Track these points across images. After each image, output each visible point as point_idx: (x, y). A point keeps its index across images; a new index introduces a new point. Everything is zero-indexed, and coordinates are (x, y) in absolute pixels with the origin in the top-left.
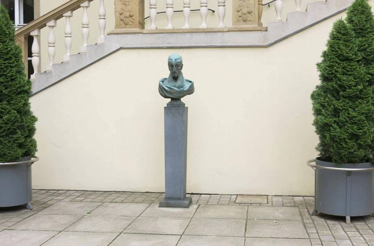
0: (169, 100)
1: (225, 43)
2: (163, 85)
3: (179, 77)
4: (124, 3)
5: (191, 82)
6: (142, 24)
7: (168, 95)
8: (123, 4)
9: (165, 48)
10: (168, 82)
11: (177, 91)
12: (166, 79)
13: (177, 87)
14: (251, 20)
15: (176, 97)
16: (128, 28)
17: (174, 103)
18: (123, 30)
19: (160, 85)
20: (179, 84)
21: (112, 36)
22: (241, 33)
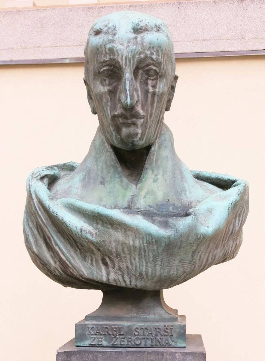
0: (97, 296)
2: (48, 203)
10: (87, 181)
12: (70, 168)
13: (148, 215)
17: (126, 324)
20: (160, 195)
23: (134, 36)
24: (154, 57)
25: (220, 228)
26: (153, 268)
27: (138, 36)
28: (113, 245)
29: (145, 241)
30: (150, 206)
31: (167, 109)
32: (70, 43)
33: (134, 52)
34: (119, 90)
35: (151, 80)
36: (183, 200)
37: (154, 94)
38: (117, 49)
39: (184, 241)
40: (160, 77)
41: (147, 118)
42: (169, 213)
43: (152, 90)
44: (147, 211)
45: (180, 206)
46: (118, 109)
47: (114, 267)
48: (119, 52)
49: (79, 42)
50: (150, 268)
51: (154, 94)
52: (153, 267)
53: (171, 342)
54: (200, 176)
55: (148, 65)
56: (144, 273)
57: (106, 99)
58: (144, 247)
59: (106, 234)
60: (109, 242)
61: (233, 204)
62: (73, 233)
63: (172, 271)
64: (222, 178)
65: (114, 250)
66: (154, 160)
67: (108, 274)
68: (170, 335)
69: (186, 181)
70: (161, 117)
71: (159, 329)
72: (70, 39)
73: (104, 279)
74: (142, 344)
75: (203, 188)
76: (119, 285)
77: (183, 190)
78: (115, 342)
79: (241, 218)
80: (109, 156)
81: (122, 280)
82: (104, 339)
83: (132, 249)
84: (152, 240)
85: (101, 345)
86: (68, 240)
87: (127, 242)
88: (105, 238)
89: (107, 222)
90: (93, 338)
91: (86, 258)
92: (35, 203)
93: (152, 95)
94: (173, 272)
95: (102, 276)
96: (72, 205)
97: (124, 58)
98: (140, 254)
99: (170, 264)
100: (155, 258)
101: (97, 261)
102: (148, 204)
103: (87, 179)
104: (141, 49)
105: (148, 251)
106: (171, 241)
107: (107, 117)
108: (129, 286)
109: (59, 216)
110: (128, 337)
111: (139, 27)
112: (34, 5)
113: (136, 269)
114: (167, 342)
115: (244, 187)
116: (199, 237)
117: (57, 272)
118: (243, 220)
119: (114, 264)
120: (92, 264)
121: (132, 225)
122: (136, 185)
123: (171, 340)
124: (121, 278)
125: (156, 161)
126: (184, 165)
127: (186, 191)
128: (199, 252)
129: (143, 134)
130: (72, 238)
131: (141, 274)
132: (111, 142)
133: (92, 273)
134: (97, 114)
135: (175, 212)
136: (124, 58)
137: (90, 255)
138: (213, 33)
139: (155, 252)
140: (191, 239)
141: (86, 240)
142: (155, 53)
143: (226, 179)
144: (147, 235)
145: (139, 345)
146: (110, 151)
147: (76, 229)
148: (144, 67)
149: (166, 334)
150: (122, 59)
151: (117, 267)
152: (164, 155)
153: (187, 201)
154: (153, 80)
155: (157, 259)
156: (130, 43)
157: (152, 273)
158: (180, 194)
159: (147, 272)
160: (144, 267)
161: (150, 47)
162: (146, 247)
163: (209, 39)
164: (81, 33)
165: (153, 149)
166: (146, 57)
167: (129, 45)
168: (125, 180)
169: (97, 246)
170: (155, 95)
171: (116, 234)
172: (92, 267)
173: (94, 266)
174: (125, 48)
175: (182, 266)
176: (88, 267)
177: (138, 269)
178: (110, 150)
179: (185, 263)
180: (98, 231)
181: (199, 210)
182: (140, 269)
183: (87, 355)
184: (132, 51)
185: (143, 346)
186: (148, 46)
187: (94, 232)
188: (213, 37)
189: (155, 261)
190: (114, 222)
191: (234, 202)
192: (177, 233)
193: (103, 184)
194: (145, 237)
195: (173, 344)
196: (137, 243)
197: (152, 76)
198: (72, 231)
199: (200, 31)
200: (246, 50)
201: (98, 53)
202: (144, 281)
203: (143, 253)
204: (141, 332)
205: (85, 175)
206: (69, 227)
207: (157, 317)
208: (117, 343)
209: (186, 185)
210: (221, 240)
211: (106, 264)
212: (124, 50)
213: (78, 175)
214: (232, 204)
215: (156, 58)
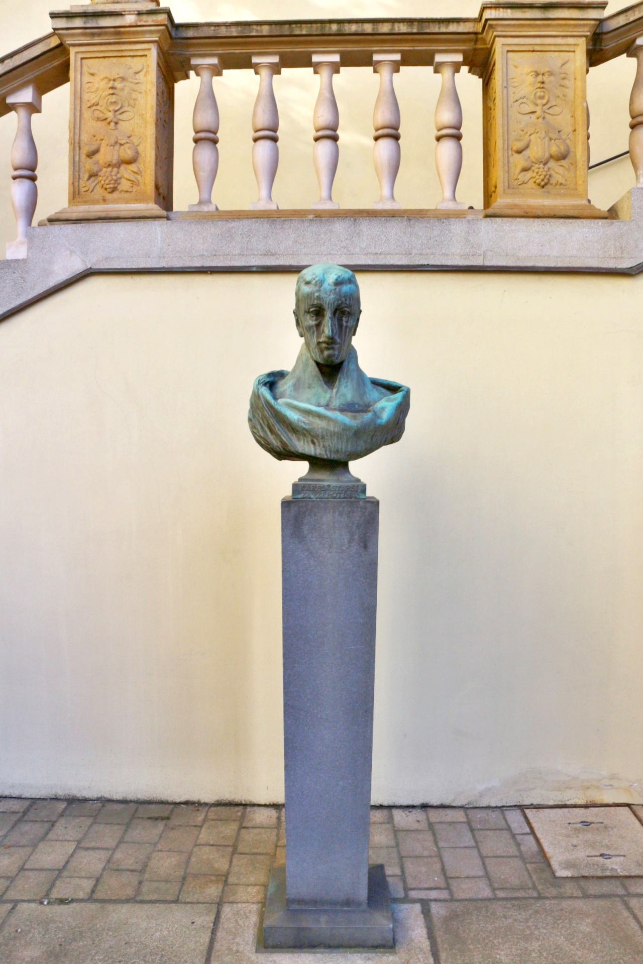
0: (303, 467)
1: (482, 257)
3: (346, 363)
4: (101, 115)
5: (393, 388)
6: (164, 198)
7: (303, 446)
8: (98, 119)
9: (254, 269)
11: (346, 428)
12: (281, 375)
13: (342, 410)
14: (561, 184)
15: (334, 456)
16: (116, 201)
17: (326, 483)
18: (98, 209)
19: (256, 397)
21: (56, 228)
22: (537, 224)
23: (334, 288)
24: (348, 302)
28: (320, 430)
29: (341, 429)
30: (342, 404)
31: (354, 334)
37: (346, 327)
40: (351, 314)
47: (319, 446)
48: (324, 299)
51: (346, 327)
53: (357, 496)
55: (343, 308)
65: (320, 434)
67: (315, 450)
73: (313, 453)
76: (323, 457)
78: (320, 495)
80: (313, 369)
87: (329, 428)
94: (359, 448)
95: (311, 451)
96: (290, 404)
97: (327, 303)
98: (338, 437)
101: (308, 442)
110: (327, 492)
111: (338, 282)
112: (217, 209)
117: (278, 448)
120: (304, 443)
122: (332, 389)
124: (324, 453)
125: (346, 373)
129: (338, 355)
132: (315, 359)
133: (304, 450)
136: (327, 303)
140: (372, 427)
142: (348, 300)
148: (341, 309)
149: (353, 490)
150: (326, 303)
151: (322, 446)
154: (346, 317)
159: (341, 449)
165: (344, 364)
166: (342, 303)
177: (336, 447)
178: (314, 364)
188: (384, 251)
189: (347, 441)
195: (358, 496)
196: (336, 430)
204: (337, 490)
205: (296, 382)
208: (322, 495)
209: (367, 390)
211: (314, 443)
212: (327, 297)
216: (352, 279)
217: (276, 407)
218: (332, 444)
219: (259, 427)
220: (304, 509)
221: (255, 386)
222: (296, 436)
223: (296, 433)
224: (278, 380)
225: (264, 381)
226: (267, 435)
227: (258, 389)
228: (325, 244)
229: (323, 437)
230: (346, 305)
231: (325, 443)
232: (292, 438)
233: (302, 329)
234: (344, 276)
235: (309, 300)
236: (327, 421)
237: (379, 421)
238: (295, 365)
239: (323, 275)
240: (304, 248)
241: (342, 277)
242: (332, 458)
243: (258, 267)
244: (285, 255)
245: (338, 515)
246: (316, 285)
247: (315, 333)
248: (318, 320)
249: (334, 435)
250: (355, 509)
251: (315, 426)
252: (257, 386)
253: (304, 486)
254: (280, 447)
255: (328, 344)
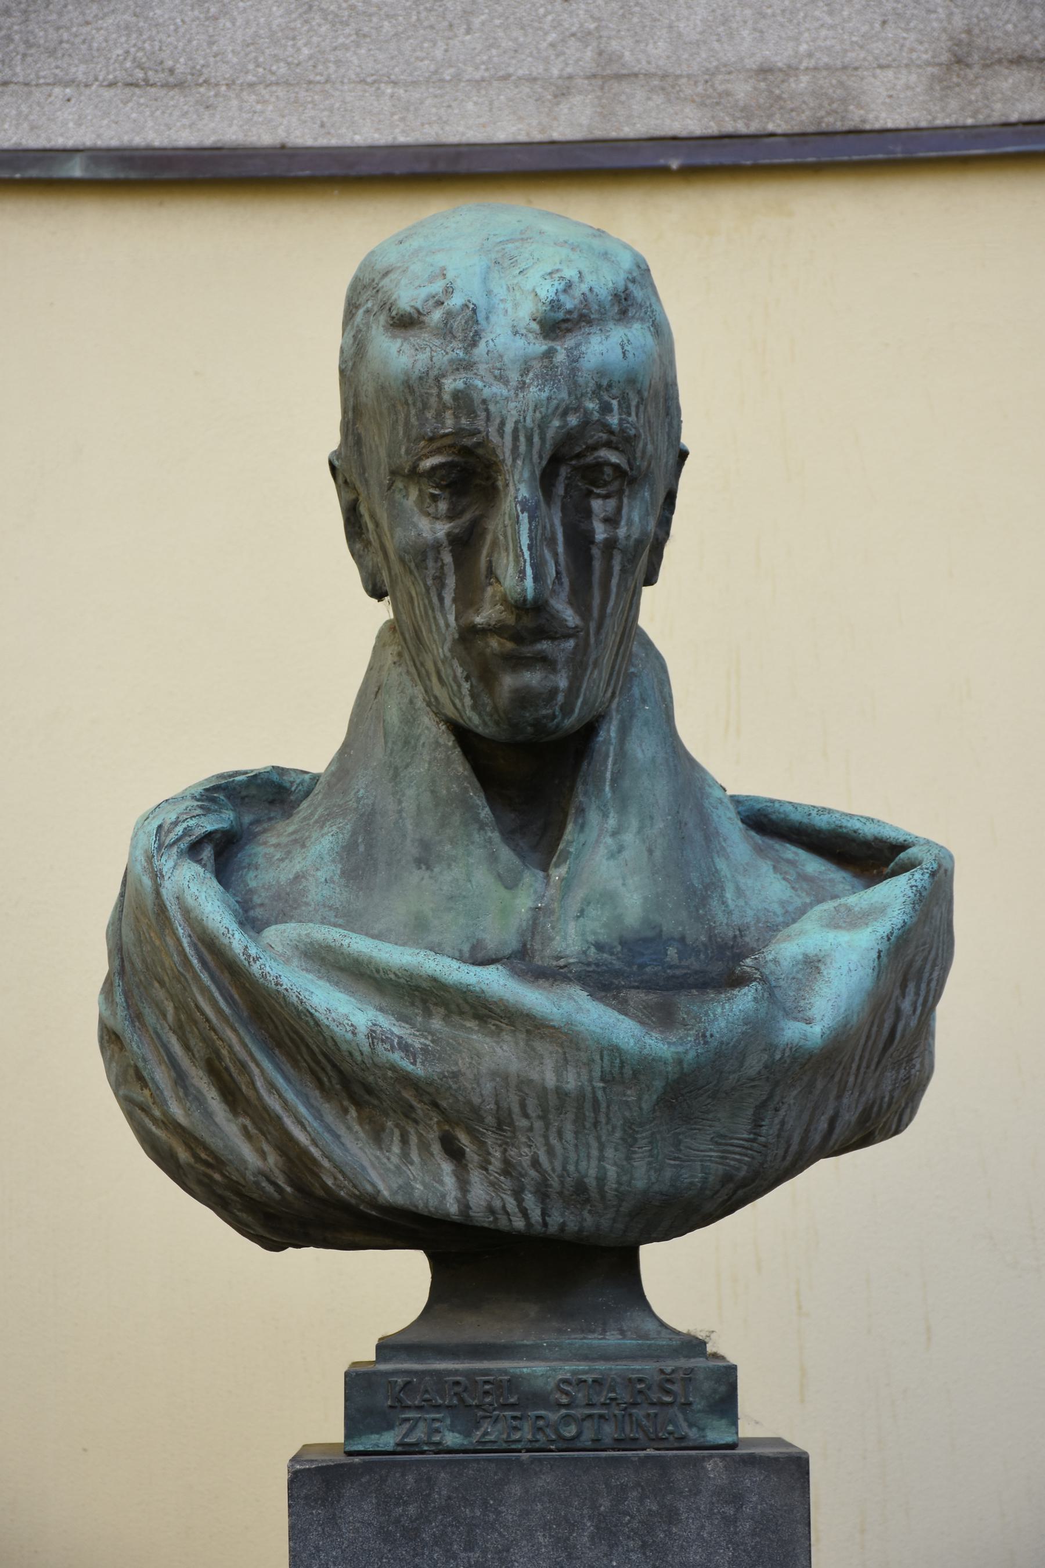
9: (76, 170)
23: (540, 347)
24: (614, 420)
25: (849, 1026)
26: (623, 1166)
27: (559, 348)
28: (488, 1087)
29: (597, 1074)
30: (600, 947)
31: (650, 579)
32: (82, 68)
33: (543, 410)
34: (489, 538)
35: (599, 496)
36: (715, 923)
38: (484, 397)
39: (729, 1073)
40: (632, 481)
41: (588, 634)
42: (668, 971)
43: (605, 536)
44: (589, 964)
45: (704, 945)
46: (487, 605)
48: (492, 408)
49: (128, 64)
50: (615, 1164)
51: (611, 544)
52: (625, 1163)
53: (685, 1429)
54: (770, 820)
56: (591, 1182)
57: (440, 564)
58: (594, 1092)
59: (460, 1052)
60: (471, 1077)
61: (893, 939)
62: (339, 1049)
63: (686, 1176)
64: (855, 832)
66: (608, 775)
68: (684, 1404)
69: (723, 848)
70: (630, 619)
71: (640, 1380)
72: (84, 47)
73: (453, 1208)
74: (583, 1438)
75: (786, 873)
76: (503, 1223)
77: (713, 884)
79: (923, 986)
81: (517, 1210)
82: (448, 1422)
83: (553, 1101)
84: (622, 1067)
85: (439, 1443)
86: (313, 1072)
87: (535, 1076)
88: (457, 1064)
89: (467, 1008)
90: (407, 1420)
91: (383, 1136)
92: (185, 942)
93: (603, 552)
94: (692, 1176)
96: (329, 948)
97: (509, 428)
98: (579, 1120)
99: (680, 1150)
100: (631, 1131)
101: (424, 1147)
102: (591, 938)
103: (362, 848)
104: (570, 394)
105: (608, 1107)
106: (685, 1070)
107: (443, 629)
108: (539, 1228)
109: (286, 990)
110: (532, 1413)
111: (561, 315)
113: (564, 1169)
114: (670, 1428)
115: (933, 874)
116: (778, 1057)
117: (270, 1189)
118: (932, 993)
119: (489, 1154)
120: (405, 1155)
121: (552, 1020)
122: (545, 868)
123: (686, 1420)
124: (511, 1204)
126: (710, 786)
127: (723, 889)
128: (777, 1110)
129: (573, 690)
130: (334, 1066)
131: (581, 1188)
132: (450, 711)
133: (407, 1188)
134: (387, 598)
135: (688, 967)
136: (509, 428)
137: (397, 1126)
138: (808, 30)
139: (631, 1109)
140: (754, 1064)
141: (390, 1073)
142: (615, 403)
143: (870, 837)
144: (605, 1052)
145: (573, 1439)
146: (446, 745)
147: (354, 1033)
148: (579, 456)
149: (668, 1399)
151: (496, 1164)
152: (640, 755)
153: (727, 924)
155: (637, 1132)
156: (531, 375)
157: (619, 1183)
158: (704, 901)
159: (601, 1180)
160: (594, 1163)
161: (599, 386)
162: (600, 1094)
163: (789, 67)
164: (135, 15)
165: (602, 736)
166: (586, 423)
167: (527, 381)
168: (506, 854)
169: (428, 1093)
170: (614, 548)
171: (498, 1050)
172: (404, 1168)
173: (412, 1163)
174: (512, 392)
175: (722, 1157)
176: (392, 1167)
177: (571, 1168)
178: (448, 740)
179: (732, 1145)
180: (433, 1041)
181: (775, 961)
182: (577, 1170)
183: (397, 1475)
184: (536, 406)
185: (589, 1444)
186: (592, 384)
187: (417, 1045)
188: (810, 55)
189: (629, 1142)
190: (491, 1010)
191: (896, 931)
192: (706, 1043)
193: (424, 867)
194: (597, 1057)
196: (571, 1082)
197: (606, 484)
198: (338, 1040)
199: (745, 22)
200: (970, 121)
201: (410, 402)
202: (590, 1212)
203: (589, 1114)
205: (354, 833)
206: (328, 1027)
207: (634, 1342)
209: (721, 864)
210: (854, 1066)
211: (454, 1152)
212: (507, 399)
213: (326, 830)
214: (889, 939)
215: (621, 420)
216: (638, 293)
217: (255, 968)
218: (551, 1152)
219: (161, 1076)
220: (412, 1510)
221: (142, 858)
222: (361, 1121)
223: (358, 1104)
224: (257, 822)
225: (187, 832)
226: (208, 1115)
227: (157, 876)
228: (477, 22)
229: (503, 1123)
230: (605, 436)
231: (512, 1152)
232: (342, 1131)
233: (380, 559)
234: (590, 280)
235: (413, 412)
236: (523, 1036)
237: (792, 1031)
238: (346, 746)
239: (485, 280)
240: (358, 45)
241: (584, 288)
242: (553, 1229)
243: (96, 155)
244: (251, 85)
245: (592, 1538)
246: (446, 331)
247: (451, 581)
248: (462, 513)
249: (560, 1109)
250: (681, 1506)
251: (463, 1063)
252: (150, 859)
253: (407, 1384)
254: (281, 1181)
255: (518, 638)
